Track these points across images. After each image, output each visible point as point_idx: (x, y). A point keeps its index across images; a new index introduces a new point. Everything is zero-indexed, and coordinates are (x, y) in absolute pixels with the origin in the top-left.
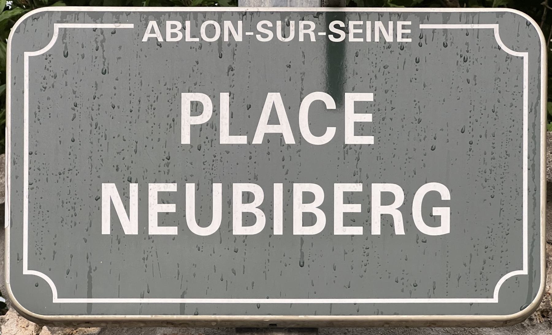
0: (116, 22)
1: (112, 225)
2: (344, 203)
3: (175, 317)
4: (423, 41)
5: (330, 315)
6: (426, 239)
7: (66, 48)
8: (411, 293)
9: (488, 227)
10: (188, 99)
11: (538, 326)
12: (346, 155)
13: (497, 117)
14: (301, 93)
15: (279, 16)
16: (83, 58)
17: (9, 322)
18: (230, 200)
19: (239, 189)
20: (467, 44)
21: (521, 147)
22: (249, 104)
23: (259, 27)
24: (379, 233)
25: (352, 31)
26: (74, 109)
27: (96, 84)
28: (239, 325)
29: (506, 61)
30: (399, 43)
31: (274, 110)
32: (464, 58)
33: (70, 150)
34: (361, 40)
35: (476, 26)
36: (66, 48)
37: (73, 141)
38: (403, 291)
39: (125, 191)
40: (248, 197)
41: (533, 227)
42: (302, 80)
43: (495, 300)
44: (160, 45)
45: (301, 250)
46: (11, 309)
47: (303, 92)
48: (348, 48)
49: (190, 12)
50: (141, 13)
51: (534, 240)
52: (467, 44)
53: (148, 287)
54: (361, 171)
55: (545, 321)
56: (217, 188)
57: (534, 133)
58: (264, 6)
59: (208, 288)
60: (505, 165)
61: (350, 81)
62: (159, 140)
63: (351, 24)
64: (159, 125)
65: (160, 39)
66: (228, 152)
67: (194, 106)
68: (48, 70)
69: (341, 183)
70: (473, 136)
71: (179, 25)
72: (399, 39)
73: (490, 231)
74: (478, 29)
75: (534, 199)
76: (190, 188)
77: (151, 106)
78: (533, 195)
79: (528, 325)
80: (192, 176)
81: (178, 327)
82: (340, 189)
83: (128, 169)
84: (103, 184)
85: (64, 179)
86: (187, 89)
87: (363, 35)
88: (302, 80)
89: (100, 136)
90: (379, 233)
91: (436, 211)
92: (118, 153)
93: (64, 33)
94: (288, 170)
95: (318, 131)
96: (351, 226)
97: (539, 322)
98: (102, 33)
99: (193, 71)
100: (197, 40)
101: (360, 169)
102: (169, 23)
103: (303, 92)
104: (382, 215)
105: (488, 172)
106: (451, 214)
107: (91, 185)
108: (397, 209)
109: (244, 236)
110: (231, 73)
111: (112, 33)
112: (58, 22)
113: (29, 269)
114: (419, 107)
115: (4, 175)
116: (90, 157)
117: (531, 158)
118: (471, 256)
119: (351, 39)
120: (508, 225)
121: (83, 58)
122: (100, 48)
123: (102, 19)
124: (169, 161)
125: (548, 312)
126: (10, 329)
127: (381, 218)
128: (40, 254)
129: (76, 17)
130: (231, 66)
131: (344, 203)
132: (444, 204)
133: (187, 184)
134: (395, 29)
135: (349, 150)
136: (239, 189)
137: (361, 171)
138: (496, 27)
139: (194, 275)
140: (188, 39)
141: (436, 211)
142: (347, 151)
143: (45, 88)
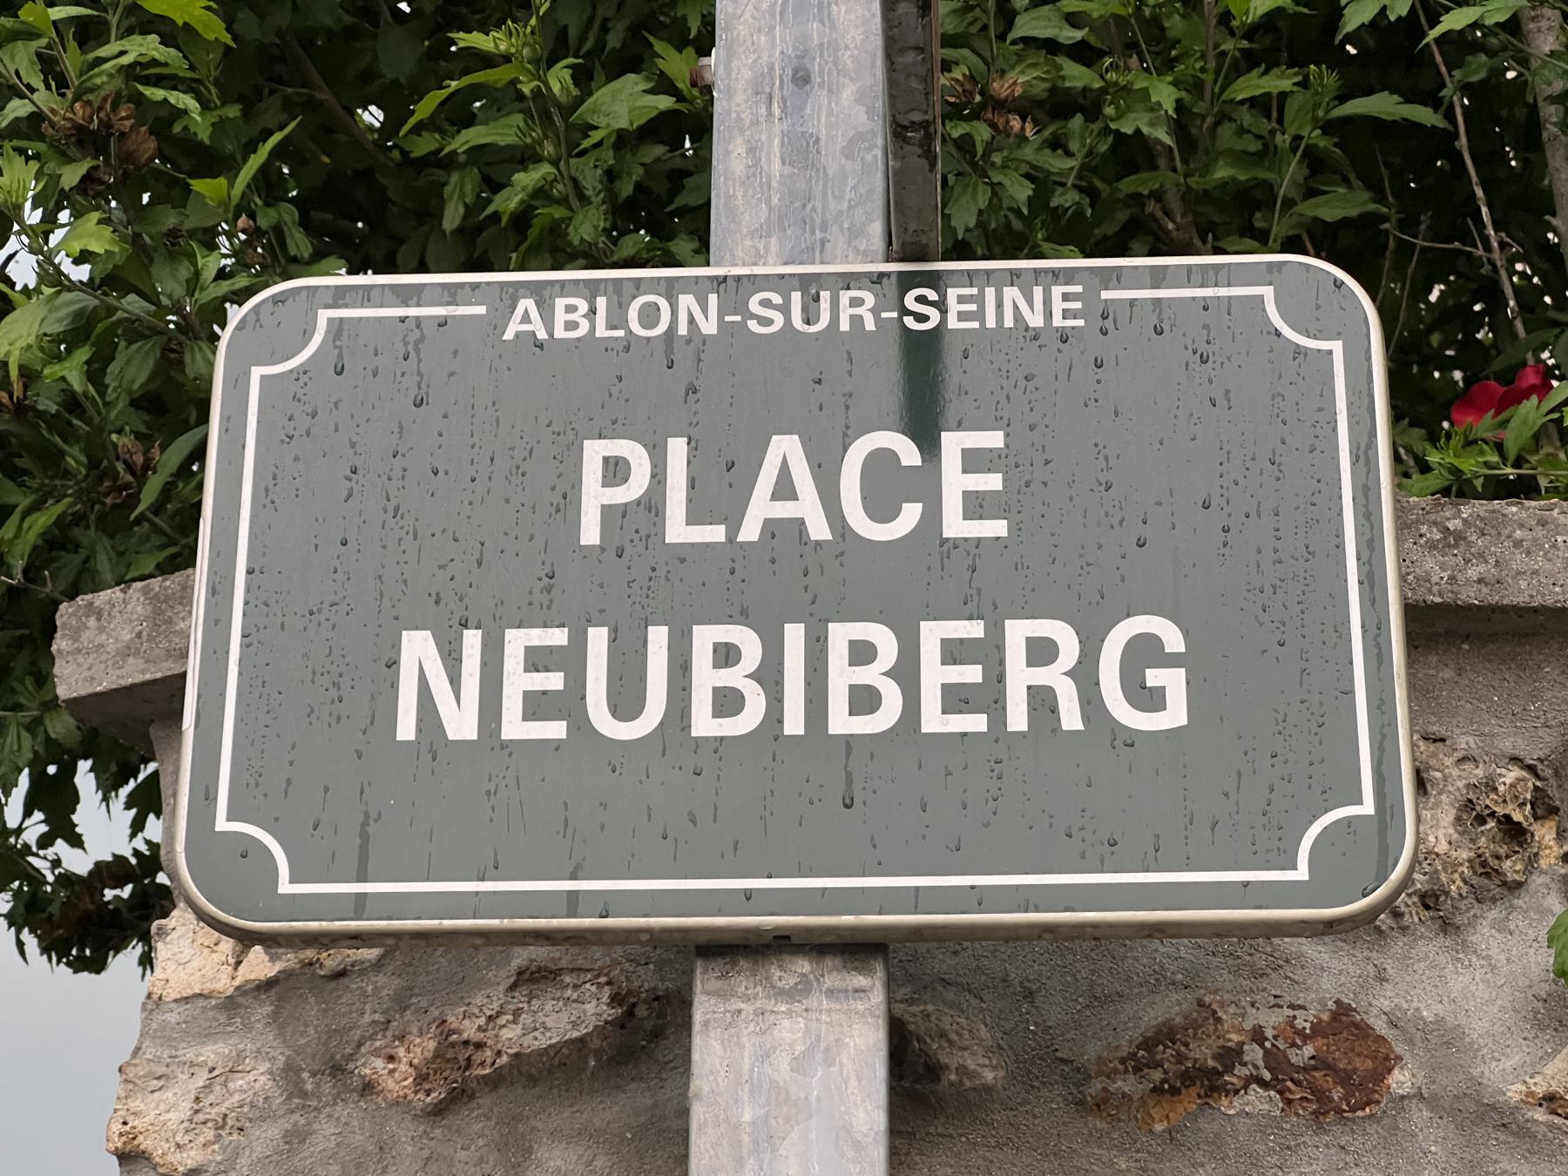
0: (449, 304)
1: (419, 720)
2: (943, 663)
3: (555, 923)
4: (1109, 323)
5: (916, 913)
6: (1132, 739)
7: (340, 356)
8: (1102, 862)
9: (1276, 711)
10: (597, 453)
11: (1415, 930)
12: (946, 560)
13: (1281, 475)
14: (845, 435)
15: (795, 282)
16: (375, 375)
17: (174, 935)
18: (686, 662)
19: (705, 637)
20: (1206, 327)
21: (1340, 535)
22: (729, 459)
23: (754, 305)
24: (1024, 728)
25: (954, 307)
26: (350, 479)
27: (401, 427)
28: (702, 939)
29: (1295, 359)
30: (1057, 329)
31: (785, 469)
32: (1202, 356)
33: (336, 563)
34: (976, 325)
35: (1223, 292)
36: (340, 356)
37: (344, 543)
38: (1083, 856)
39: (453, 646)
40: (726, 655)
41: (1379, 708)
42: (847, 407)
43: (1302, 873)
44: (540, 345)
45: (846, 766)
46: (182, 905)
47: (849, 432)
48: (947, 340)
49: (607, 280)
50: (502, 284)
51: (1384, 737)
52: (1206, 327)
53: (496, 854)
54: (979, 595)
55: (1432, 918)
56: (658, 637)
57: (1366, 506)
58: (764, 264)
59: (633, 855)
60: (1307, 575)
61: (953, 406)
62: (532, 538)
63: (952, 294)
64: (533, 508)
65: (542, 335)
66: (683, 561)
67: (611, 467)
68: (299, 401)
69: (935, 619)
70: (1229, 515)
71: (583, 306)
72: (1058, 321)
73: (1281, 718)
74: (1230, 297)
75: (1378, 645)
76: (598, 639)
77: (518, 468)
78: (1375, 639)
79: (1393, 929)
80: (602, 611)
81: (560, 944)
82: (932, 634)
83: (461, 600)
84: (404, 633)
85: (319, 624)
86: (596, 431)
87: (980, 315)
88: (847, 407)
89: (403, 532)
90: (1024, 728)
91: (1154, 677)
92: (440, 567)
93: (337, 327)
94: (816, 596)
95: (881, 511)
96: (961, 712)
97: (1416, 919)
98: (418, 326)
99: (610, 395)
100: (620, 333)
101: (979, 590)
102: (560, 303)
103: (849, 432)
104: (1029, 688)
105: (1269, 590)
106: (1188, 683)
107: (377, 635)
108: (1064, 674)
109: (716, 738)
110: (692, 397)
111: (440, 325)
112: (327, 307)
113: (231, 817)
114: (1106, 458)
115: (190, 612)
116: (380, 577)
117: (1365, 559)
118: (1239, 774)
119: (953, 323)
120: (1322, 704)
121: (375, 375)
122: (413, 355)
123: (419, 299)
124: (551, 581)
125: (1437, 898)
126: (175, 950)
127: (1029, 694)
128: (257, 785)
129: (366, 296)
130: (691, 383)
131: (943, 663)
132: (1172, 661)
133: (590, 630)
134: (1047, 302)
135: (952, 551)
136: (705, 637)
137: (979, 595)
138: (1268, 292)
139: (602, 827)
140: (602, 332)
141: (1154, 677)
142: (949, 552)
143: (291, 438)
